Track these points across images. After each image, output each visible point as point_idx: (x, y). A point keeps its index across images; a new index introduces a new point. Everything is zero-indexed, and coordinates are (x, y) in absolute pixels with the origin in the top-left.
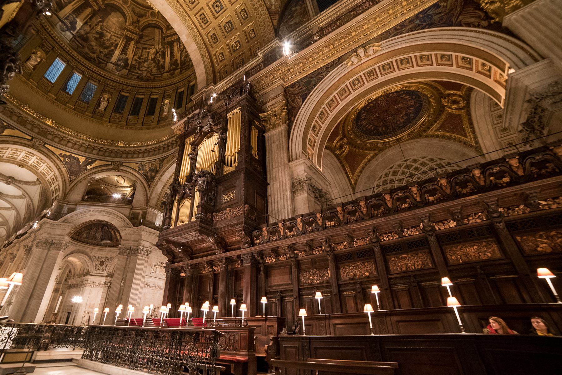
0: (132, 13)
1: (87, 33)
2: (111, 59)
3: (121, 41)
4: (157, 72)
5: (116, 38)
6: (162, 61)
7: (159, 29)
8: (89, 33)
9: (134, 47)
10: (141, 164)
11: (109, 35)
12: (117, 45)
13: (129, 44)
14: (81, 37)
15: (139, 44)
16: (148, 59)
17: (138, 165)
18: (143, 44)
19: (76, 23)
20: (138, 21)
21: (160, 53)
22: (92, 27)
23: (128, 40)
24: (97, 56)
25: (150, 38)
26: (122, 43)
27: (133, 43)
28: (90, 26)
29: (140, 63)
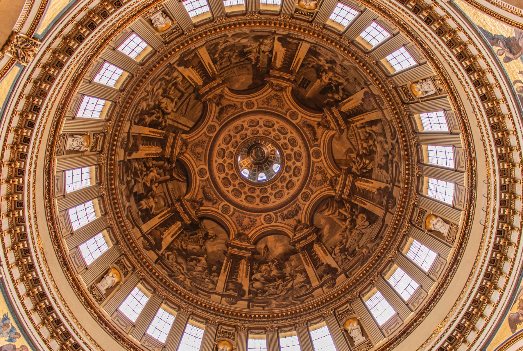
0: (232, 103)
1: (262, 43)
2: (206, 48)
3: (215, 70)
4: (139, 110)
5: (222, 67)
6: (148, 120)
7: (191, 129)
8: (259, 45)
9: (194, 82)
11: (233, 61)
12: (215, 62)
13: (202, 78)
14: (265, 37)
16: (164, 97)
19: (283, 46)
20: (218, 104)
21: (160, 120)
22: (261, 53)
24: (227, 36)
25: (189, 108)
26: (212, 69)
27: (200, 82)
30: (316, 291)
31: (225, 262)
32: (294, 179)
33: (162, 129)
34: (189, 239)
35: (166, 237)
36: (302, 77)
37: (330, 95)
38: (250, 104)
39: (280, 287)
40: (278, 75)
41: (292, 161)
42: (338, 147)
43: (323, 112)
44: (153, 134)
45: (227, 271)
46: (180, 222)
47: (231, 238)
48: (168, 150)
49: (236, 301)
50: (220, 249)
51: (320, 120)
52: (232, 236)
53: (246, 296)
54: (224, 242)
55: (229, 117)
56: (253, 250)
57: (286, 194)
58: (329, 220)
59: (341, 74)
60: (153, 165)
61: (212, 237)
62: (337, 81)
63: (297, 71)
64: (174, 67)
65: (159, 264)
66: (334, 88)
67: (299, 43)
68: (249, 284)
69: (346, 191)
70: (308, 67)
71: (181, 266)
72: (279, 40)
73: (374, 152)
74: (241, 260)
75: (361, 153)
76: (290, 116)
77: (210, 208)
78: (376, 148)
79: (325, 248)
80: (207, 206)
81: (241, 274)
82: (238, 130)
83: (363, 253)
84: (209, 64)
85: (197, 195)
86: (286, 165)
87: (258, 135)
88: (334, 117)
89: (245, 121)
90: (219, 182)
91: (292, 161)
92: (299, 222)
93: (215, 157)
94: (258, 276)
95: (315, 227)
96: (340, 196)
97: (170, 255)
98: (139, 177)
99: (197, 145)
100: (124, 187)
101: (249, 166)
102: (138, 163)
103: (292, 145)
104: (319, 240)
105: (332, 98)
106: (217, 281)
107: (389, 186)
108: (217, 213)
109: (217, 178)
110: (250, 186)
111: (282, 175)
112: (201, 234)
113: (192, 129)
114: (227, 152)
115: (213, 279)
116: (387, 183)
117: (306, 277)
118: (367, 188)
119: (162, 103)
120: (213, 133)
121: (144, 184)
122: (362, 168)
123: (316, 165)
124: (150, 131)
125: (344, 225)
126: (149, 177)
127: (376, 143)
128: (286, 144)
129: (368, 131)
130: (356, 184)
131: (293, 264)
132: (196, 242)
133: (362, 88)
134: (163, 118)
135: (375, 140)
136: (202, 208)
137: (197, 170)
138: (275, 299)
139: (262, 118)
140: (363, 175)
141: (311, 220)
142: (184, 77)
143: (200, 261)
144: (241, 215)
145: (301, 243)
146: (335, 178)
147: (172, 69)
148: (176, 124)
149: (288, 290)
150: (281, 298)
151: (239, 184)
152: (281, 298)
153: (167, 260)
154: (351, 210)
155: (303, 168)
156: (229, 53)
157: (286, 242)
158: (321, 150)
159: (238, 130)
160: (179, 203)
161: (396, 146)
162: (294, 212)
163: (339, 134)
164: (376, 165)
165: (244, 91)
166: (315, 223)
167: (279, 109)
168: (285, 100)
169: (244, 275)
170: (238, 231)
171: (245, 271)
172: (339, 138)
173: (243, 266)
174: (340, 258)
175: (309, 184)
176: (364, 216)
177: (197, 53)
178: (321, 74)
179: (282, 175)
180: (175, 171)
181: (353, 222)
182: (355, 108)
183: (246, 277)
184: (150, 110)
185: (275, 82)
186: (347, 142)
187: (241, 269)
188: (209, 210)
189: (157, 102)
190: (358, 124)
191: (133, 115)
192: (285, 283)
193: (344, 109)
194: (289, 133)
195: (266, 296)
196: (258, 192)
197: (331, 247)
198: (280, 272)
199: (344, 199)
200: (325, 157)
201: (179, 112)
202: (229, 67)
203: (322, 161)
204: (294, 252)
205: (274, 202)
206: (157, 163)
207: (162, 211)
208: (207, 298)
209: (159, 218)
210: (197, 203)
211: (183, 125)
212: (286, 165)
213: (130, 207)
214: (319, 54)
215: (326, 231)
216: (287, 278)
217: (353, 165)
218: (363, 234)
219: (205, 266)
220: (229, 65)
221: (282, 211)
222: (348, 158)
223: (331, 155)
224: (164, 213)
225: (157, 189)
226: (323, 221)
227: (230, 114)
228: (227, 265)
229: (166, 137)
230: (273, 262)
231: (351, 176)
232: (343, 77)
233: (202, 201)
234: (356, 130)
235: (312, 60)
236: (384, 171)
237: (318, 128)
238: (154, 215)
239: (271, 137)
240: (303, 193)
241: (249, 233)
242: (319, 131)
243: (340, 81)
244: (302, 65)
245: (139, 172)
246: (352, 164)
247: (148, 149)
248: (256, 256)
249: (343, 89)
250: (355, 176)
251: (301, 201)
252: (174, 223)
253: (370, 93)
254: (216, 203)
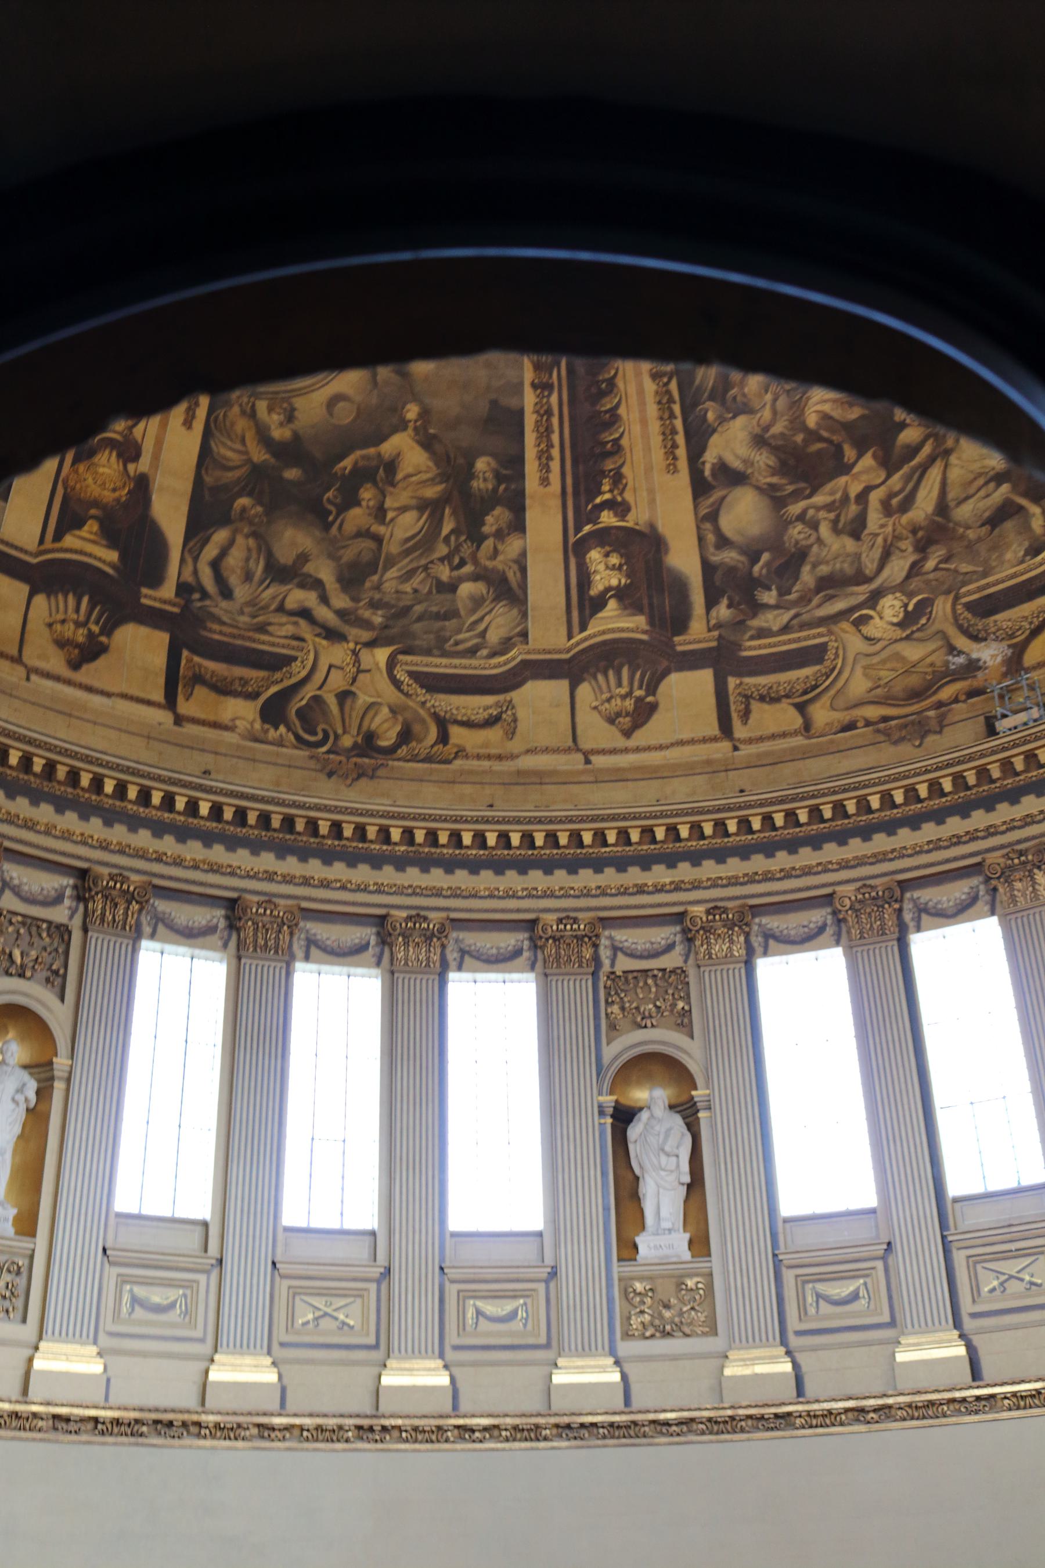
31: (530, 399)
39: (874, 518)
49: (652, 690)
97: (224, 553)
106: (521, 563)
115: (498, 564)
143: (391, 466)
150: (891, 607)
152: (891, 607)
153: (224, 604)
169: (658, 455)
171: (655, 427)
183: (672, 468)
195: (805, 599)
208: (494, 734)
219: (431, 492)
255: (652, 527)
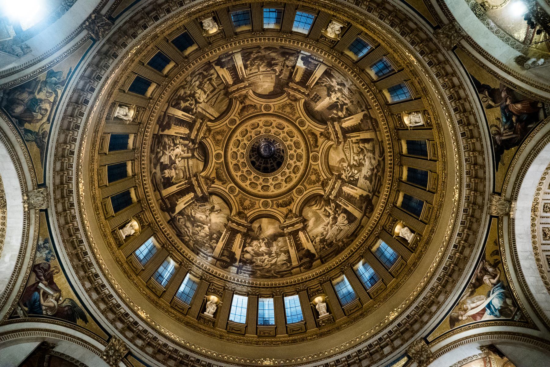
0: (253, 104)
1: (287, 59)
2: (241, 54)
3: (245, 74)
5: (251, 72)
6: (183, 105)
8: (285, 60)
9: (226, 80)
10: (62, 84)
11: (261, 69)
12: (246, 67)
14: (292, 55)
15: (223, 88)
16: (199, 88)
17: (66, 72)
18: (219, 91)
20: (241, 103)
21: (193, 107)
22: (285, 67)
23: (237, 79)
24: (261, 48)
25: (218, 101)
26: (242, 73)
27: (230, 81)
28: (287, 66)
29: (205, 77)
30: (294, 270)
31: (224, 233)
32: (293, 175)
33: (192, 115)
34: (198, 208)
35: (180, 203)
36: (315, 93)
37: (335, 112)
38: (267, 108)
39: (266, 261)
40: (296, 88)
41: (294, 160)
42: (333, 156)
43: (327, 124)
44: (184, 117)
45: (224, 241)
46: (193, 194)
47: (232, 215)
48: (194, 133)
50: (221, 221)
51: (323, 130)
52: (234, 212)
53: (237, 264)
54: (226, 216)
55: (248, 115)
56: (248, 227)
57: (284, 187)
58: (315, 214)
59: (348, 96)
60: (180, 142)
61: (217, 211)
62: (343, 101)
63: (312, 87)
64: (212, 65)
65: (171, 224)
66: (339, 107)
67: (318, 64)
68: (241, 255)
69: (334, 193)
70: (321, 85)
71: (188, 229)
72: (302, 59)
73: (363, 165)
74: (238, 233)
75: (352, 164)
76: (299, 123)
77: (219, 187)
78: (365, 162)
79: (308, 236)
80: (217, 185)
81: (235, 245)
82: (255, 127)
83: (339, 246)
84: (241, 68)
85: (210, 174)
86: (288, 163)
87: (270, 134)
88: (335, 131)
89: (261, 121)
90: (231, 167)
91: (294, 160)
92: (291, 211)
93: (231, 146)
94: (249, 249)
95: (303, 217)
96: (328, 196)
97: (181, 218)
98: (167, 151)
99: (218, 133)
100: (153, 156)
101: (257, 158)
102: (168, 138)
103: (296, 147)
104: (304, 229)
105: (337, 114)
106: (215, 247)
107: (370, 194)
108: (225, 192)
109: (230, 163)
110: (256, 175)
111: (283, 170)
112: (208, 207)
113: (217, 119)
114: (241, 143)
116: (369, 192)
117: (288, 257)
118: (352, 193)
119: (197, 93)
120: (233, 125)
121: (170, 156)
122: (350, 176)
123: (313, 167)
124: (182, 115)
125: (327, 220)
126: (174, 152)
127: (366, 158)
128: (291, 146)
129: (361, 147)
130: (343, 188)
131: (280, 244)
132: (204, 212)
133: (363, 111)
134: (195, 106)
135: (365, 155)
136: (213, 185)
137: (214, 153)
138: (260, 270)
139: (275, 121)
140: (350, 182)
141: (301, 211)
142: (218, 75)
143: (204, 228)
144: (244, 197)
145: (289, 228)
146: (326, 181)
147: (210, 67)
148: (204, 113)
149: (272, 265)
151: (247, 171)
154: (335, 209)
155: (302, 168)
156: (259, 62)
157: (277, 225)
158: (320, 155)
159: (255, 127)
160: (195, 178)
161: (382, 163)
162: (288, 202)
163: (337, 145)
164: (363, 176)
165: (265, 95)
166: (303, 214)
167: (291, 116)
168: (297, 109)
169: (238, 246)
170: (239, 210)
171: (239, 243)
172: (336, 149)
173: (238, 239)
174: (319, 247)
175: (304, 181)
176: (345, 216)
177: (233, 57)
178: (331, 93)
179: (283, 170)
180: (196, 151)
181: (335, 219)
182: (353, 126)
183: (240, 248)
184: (186, 97)
185: (292, 93)
186: (342, 152)
187: (236, 240)
188: (219, 188)
189: (193, 92)
190: (354, 139)
191: (172, 98)
192: (270, 259)
193: (345, 125)
194: (296, 136)
196: (261, 180)
197: (313, 237)
198: (268, 249)
199: (331, 199)
200: (321, 162)
201: (209, 103)
202: (257, 74)
203: (318, 164)
204: (282, 235)
205: (273, 191)
206: (183, 141)
207: (180, 182)
209: (177, 187)
210: (210, 180)
211: (210, 114)
212: (288, 163)
213: (155, 173)
214: (333, 77)
215: (311, 223)
216: (272, 255)
217: (344, 173)
218: (342, 230)
219: (207, 233)
220: (257, 72)
221: (279, 199)
222: (340, 166)
223: (326, 161)
224: (181, 183)
225: (179, 163)
226: (310, 214)
227: (250, 112)
228: (225, 235)
229: (195, 122)
230: (263, 240)
231: (340, 181)
232: (349, 99)
233: (214, 180)
234: (351, 144)
235: (325, 80)
236: (368, 182)
237: (320, 137)
238: (173, 184)
239: (280, 137)
240: (298, 188)
241: (248, 213)
242: (320, 140)
243: (346, 102)
244: (317, 83)
245: (167, 146)
246: (343, 172)
247: (178, 128)
248: (250, 233)
249: (347, 109)
250: (344, 182)
251: (296, 195)
252: (188, 193)
253: (369, 115)
254: (225, 183)
255: (234, 252)
